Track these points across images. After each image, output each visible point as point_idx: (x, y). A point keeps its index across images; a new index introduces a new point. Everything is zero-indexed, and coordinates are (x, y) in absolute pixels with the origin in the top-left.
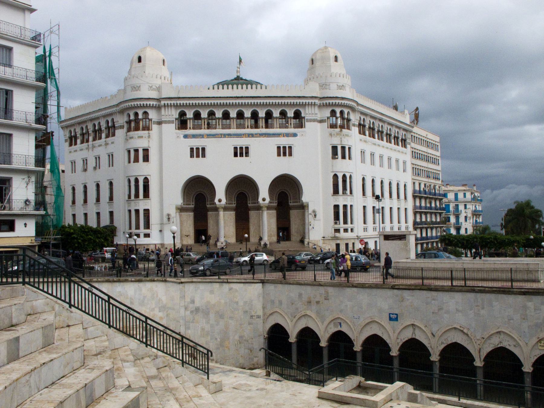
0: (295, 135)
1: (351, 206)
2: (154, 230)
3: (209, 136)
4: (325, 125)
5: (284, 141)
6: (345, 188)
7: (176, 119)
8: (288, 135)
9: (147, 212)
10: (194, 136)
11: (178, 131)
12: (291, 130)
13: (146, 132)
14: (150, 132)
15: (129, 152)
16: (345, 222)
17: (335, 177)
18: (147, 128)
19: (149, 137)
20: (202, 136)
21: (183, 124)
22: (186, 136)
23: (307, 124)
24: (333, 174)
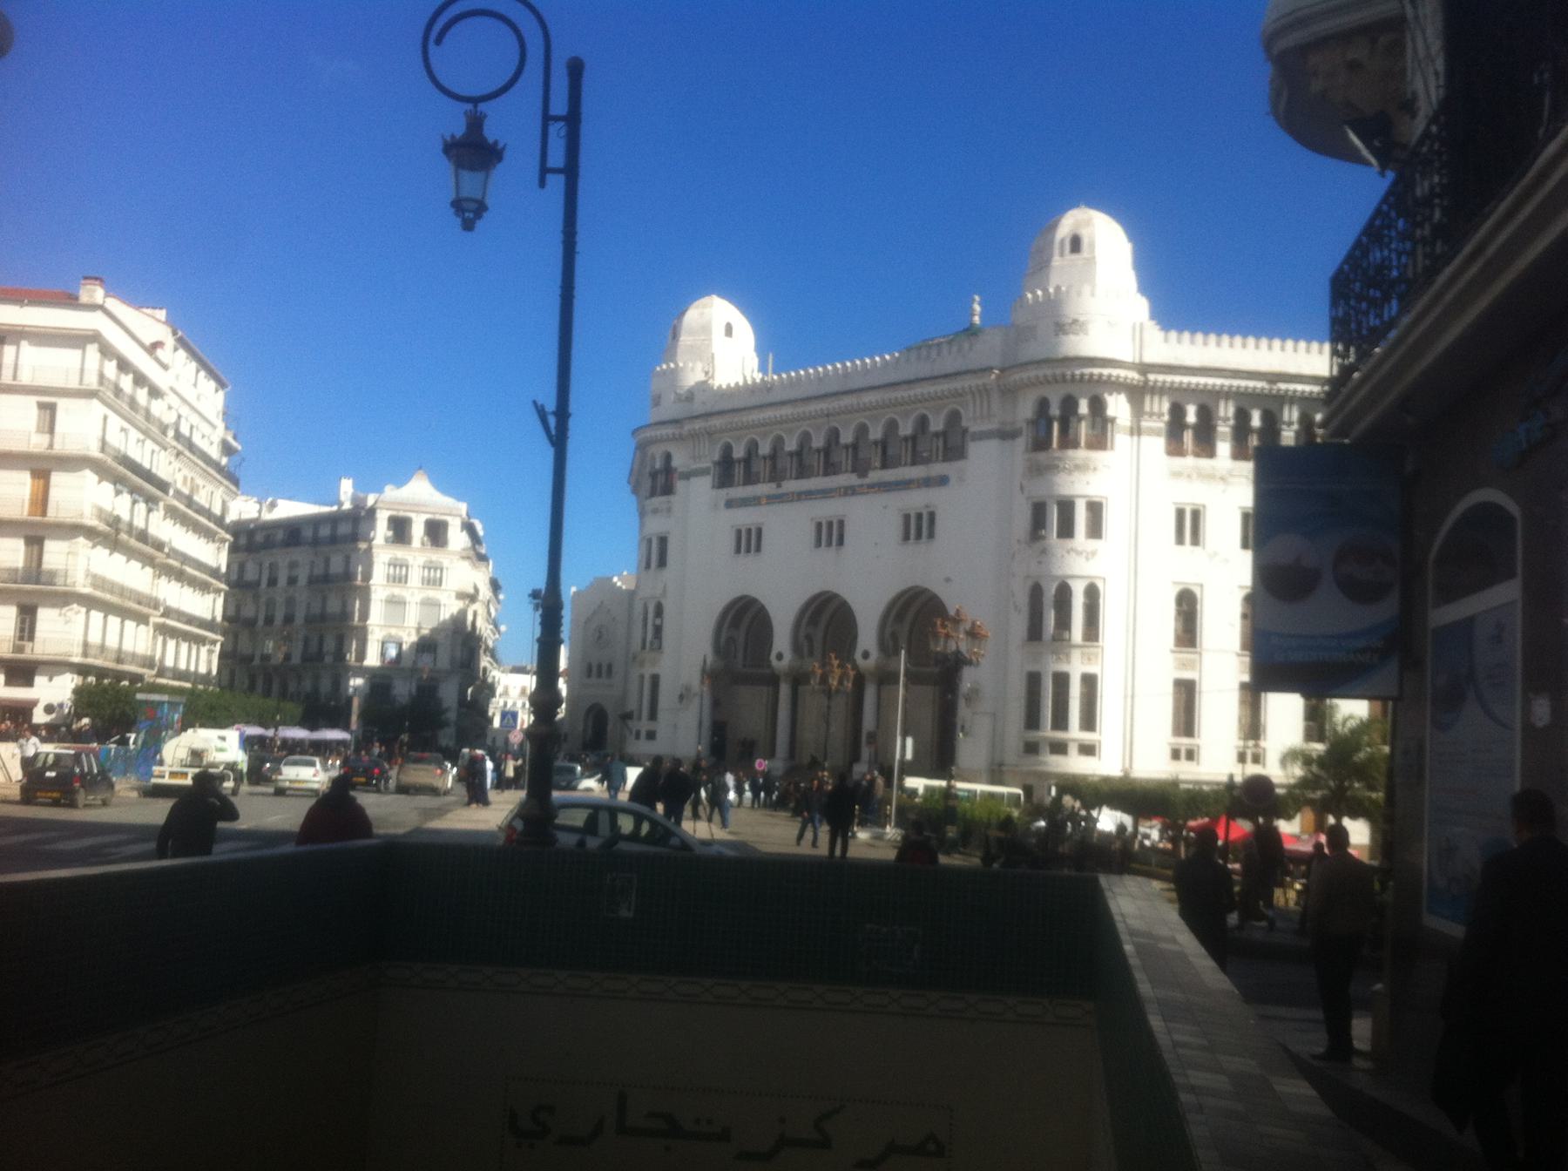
0: (943, 481)
1: (1090, 682)
2: (663, 725)
3: (773, 499)
4: (1021, 443)
5: (916, 500)
6: (1064, 622)
7: (715, 464)
8: (927, 483)
9: (655, 680)
10: (745, 502)
11: (715, 492)
12: (938, 469)
13: (663, 499)
14: (671, 498)
15: (650, 541)
16: (1061, 721)
17: (1036, 593)
18: (668, 490)
19: (669, 510)
20: (754, 501)
21: (726, 471)
22: (730, 504)
23: (975, 449)
24: (1030, 583)
